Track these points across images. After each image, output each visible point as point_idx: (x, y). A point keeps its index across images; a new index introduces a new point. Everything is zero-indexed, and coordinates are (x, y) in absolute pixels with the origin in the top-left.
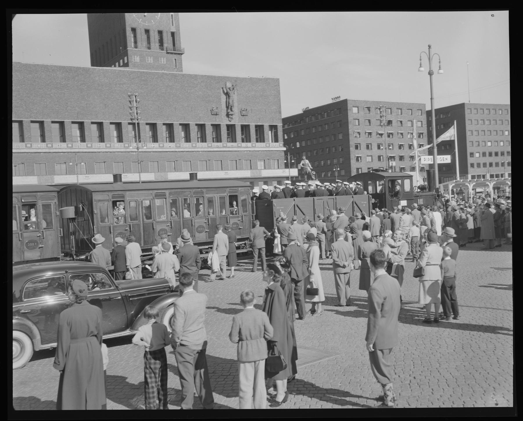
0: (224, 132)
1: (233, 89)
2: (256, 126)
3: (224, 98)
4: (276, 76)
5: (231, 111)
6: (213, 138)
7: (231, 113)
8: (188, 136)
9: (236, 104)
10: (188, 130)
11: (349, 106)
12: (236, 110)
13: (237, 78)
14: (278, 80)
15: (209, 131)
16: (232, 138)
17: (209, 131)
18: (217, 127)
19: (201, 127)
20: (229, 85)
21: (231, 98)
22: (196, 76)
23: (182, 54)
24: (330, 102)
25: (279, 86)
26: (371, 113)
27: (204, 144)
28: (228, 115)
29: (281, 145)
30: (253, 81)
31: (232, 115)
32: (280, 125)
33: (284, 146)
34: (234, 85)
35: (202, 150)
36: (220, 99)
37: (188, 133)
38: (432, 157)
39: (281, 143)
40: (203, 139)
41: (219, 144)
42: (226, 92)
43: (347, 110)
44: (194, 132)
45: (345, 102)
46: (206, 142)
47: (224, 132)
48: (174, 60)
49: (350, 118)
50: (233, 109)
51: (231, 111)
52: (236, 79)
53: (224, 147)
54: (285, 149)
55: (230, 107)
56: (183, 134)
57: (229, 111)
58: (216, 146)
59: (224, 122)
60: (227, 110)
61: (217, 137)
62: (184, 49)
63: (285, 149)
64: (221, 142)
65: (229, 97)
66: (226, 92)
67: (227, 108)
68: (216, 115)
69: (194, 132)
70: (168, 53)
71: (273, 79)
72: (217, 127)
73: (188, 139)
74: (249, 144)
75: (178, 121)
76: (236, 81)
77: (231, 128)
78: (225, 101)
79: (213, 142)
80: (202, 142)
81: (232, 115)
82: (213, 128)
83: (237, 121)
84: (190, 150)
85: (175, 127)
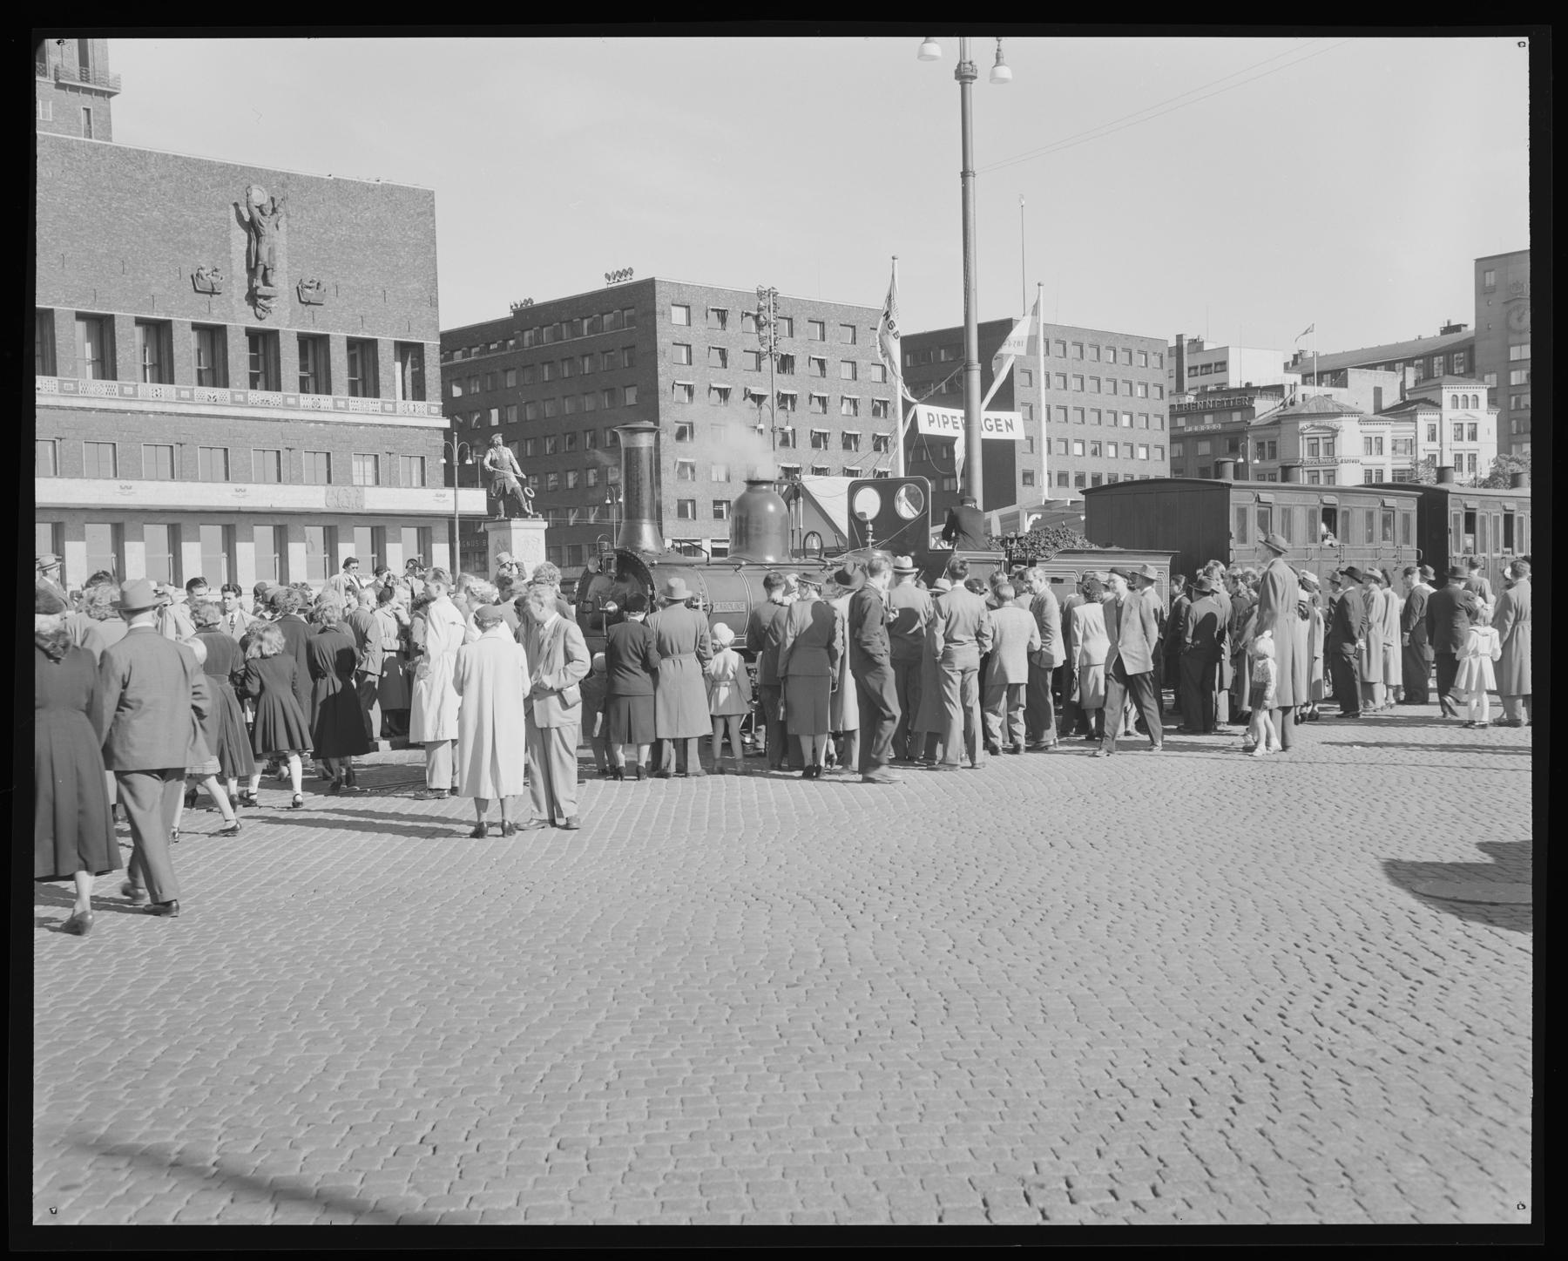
0: (238, 353)
1: (274, 210)
2: (353, 344)
3: (240, 237)
4: (424, 185)
5: (266, 283)
6: (199, 371)
7: (263, 290)
8: (108, 359)
9: (282, 264)
10: (107, 336)
11: (661, 301)
12: (282, 283)
13: (288, 176)
14: (429, 196)
15: (186, 346)
16: (265, 374)
17: (186, 346)
18: (213, 336)
19: (158, 332)
20: (259, 196)
21: (265, 240)
22: (142, 154)
23: (111, 95)
24: (601, 284)
25: (433, 215)
26: (729, 329)
27: (166, 389)
28: (252, 297)
29: (436, 410)
30: (342, 190)
31: (267, 298)
32: (432, 346)
33: (446, 413)
34: (278, 199)
35: (159, 408)
36: (228, 240)
37: (108, 348)
38: (960, 413)
39: (434, 402)
40: (163, 370)
41: (218, 392)
42: (247, 218)
43: (654, 313)
44: (131, 345)
45: (650, 285)
46: (172, 382)
47: (238, 353)
48: (83, 114)
49: (663, 341)
50: (272, 280)
51: (266, 283)
52: (287, 179)
53: (235, 403)
54: (446, 423)
55: (261, 270)
56: (88, 350)
57: (258, 282)
58: (207, 400)
59: (238, 319)
60: (250, 282)
61: (213, 370)
62: (118, 78)
63: (446, 423)
64: (226, 385)
65: (258, 235)
66: (247, 218)
67: (252, 271)
68: (212, 293)
69: (131, 345)
70: (60, 86)
71: (411, 192)
72: (213, 336)
73: (106, 367)
74: (325, 400)
75: (70, 304)
76: (284, 185)
77: (263, 342)
78: (244, 248)
79: (201, 383)
80: (160, 381)
81: (267, 298)
82: (200, 337)
83: (286, 320)
84: (113, 405)
85: (58, 322)
